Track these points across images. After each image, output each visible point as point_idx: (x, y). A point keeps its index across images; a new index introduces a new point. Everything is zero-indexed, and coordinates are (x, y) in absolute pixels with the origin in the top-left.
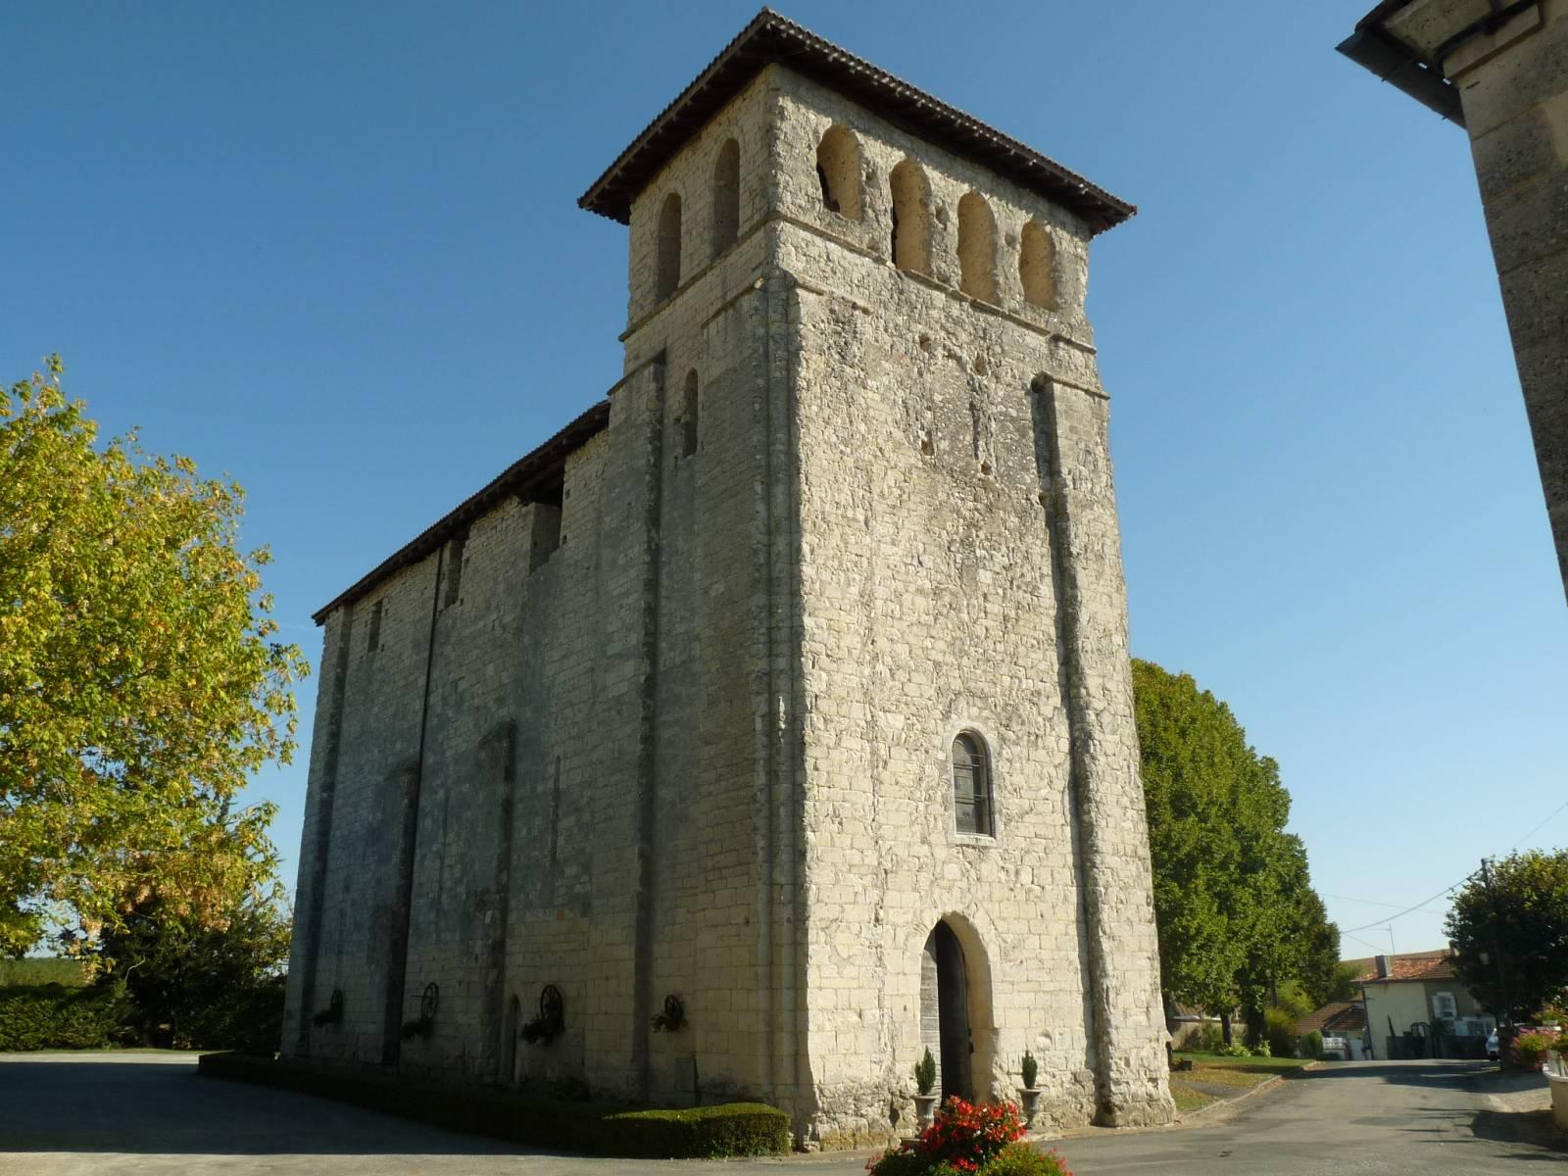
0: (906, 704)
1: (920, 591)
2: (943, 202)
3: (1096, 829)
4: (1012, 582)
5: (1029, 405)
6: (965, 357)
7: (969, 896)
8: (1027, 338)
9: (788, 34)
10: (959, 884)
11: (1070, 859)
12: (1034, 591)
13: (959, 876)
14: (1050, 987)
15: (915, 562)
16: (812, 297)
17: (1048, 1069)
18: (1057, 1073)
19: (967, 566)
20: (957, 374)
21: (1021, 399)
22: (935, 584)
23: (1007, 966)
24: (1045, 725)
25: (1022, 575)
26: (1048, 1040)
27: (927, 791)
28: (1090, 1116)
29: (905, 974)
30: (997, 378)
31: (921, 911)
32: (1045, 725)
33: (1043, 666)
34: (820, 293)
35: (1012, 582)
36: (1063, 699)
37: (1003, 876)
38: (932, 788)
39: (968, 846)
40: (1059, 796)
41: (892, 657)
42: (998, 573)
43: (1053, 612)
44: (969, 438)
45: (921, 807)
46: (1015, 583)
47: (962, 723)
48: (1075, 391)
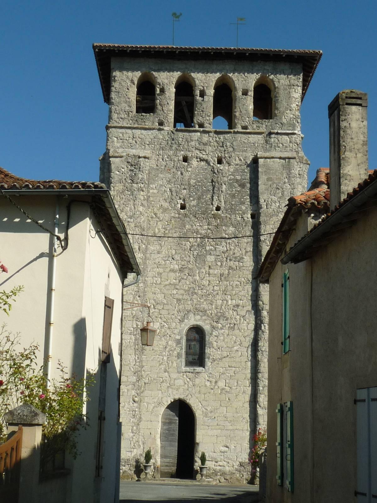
0: (160, 318)
1: (172, 271)
2: (203, 87)
3: (260, 363)
4: (227, 258)
5: (249, 172)
6: (210, 159)
7: (188, 392)
8: (250, 139)
9: (106, 50)
10: (183, 387)
11: (249, 376)
12: (240, 260)
13: (183, 384)
14: (231, 428)
15: (170, 259)
16: (117, 160)
17: (226, 460)
18: (229, 461)
19: (199, 256)
20: (206, 167)
21: (244, 170)
22: (180, 266)
23: (206, 419)
24: (240, 319)
25: (234, 254)
26: (227, 449)
27: (169, 352)
28: (247, 480)
29: (151, 421)
30: (228, 164)
31: (162, 398)
32: (240, 319)
33: (242, 293)
34: (121, 157)
35: (227, 258)
36: (252, 307)
37: (208, 384)
38: (171, 350)
39: (189, 372)
40: (246, 349)
41: (154, 300)
42: (218, 256)
43: (251, 268)
44: (209, 196)
45: (165, 358)
46: (228, 258)
47: (193, 320)
48: (272, 160)
